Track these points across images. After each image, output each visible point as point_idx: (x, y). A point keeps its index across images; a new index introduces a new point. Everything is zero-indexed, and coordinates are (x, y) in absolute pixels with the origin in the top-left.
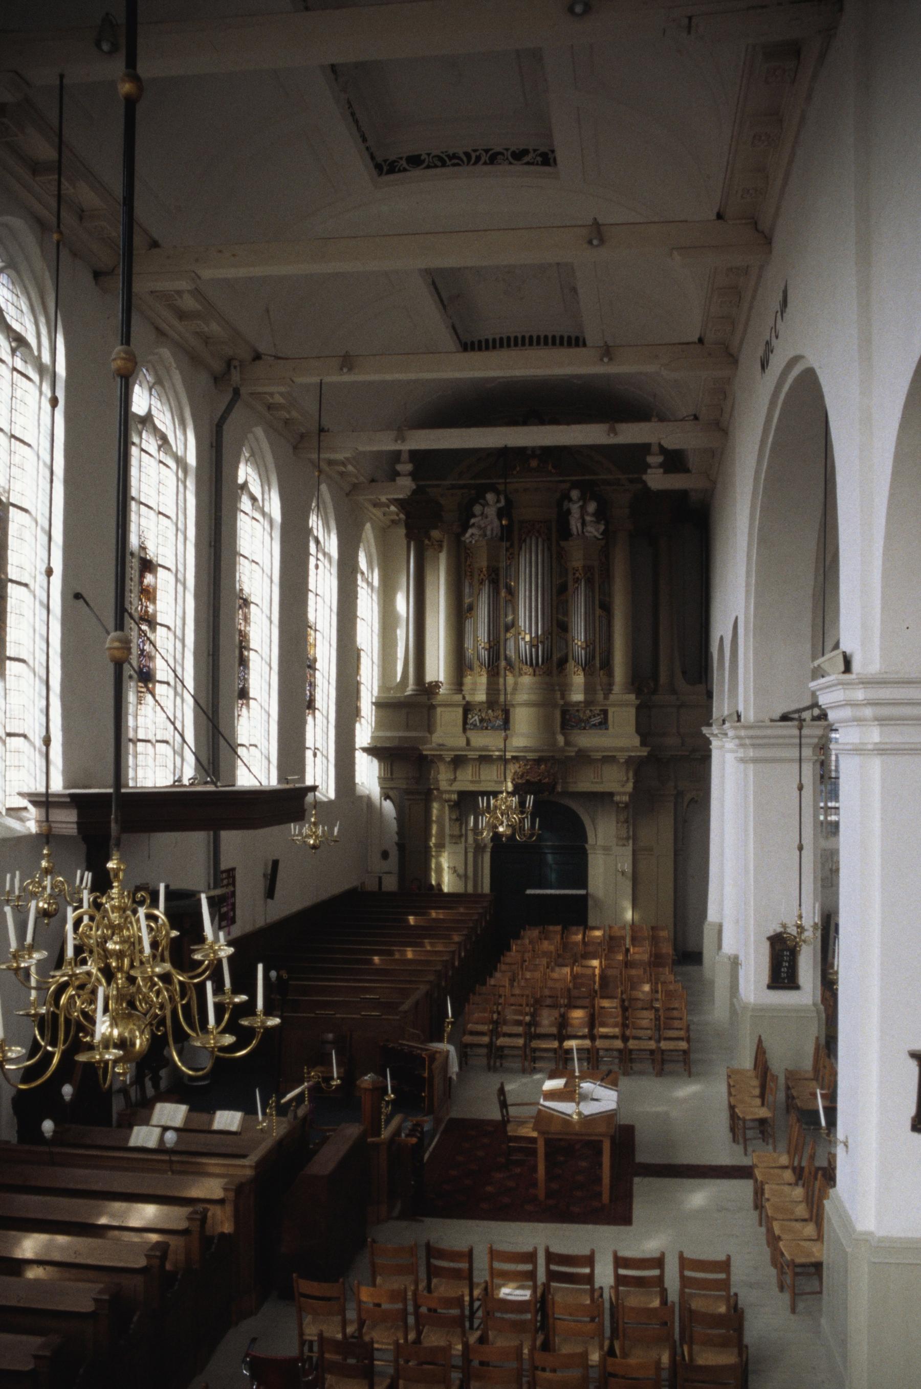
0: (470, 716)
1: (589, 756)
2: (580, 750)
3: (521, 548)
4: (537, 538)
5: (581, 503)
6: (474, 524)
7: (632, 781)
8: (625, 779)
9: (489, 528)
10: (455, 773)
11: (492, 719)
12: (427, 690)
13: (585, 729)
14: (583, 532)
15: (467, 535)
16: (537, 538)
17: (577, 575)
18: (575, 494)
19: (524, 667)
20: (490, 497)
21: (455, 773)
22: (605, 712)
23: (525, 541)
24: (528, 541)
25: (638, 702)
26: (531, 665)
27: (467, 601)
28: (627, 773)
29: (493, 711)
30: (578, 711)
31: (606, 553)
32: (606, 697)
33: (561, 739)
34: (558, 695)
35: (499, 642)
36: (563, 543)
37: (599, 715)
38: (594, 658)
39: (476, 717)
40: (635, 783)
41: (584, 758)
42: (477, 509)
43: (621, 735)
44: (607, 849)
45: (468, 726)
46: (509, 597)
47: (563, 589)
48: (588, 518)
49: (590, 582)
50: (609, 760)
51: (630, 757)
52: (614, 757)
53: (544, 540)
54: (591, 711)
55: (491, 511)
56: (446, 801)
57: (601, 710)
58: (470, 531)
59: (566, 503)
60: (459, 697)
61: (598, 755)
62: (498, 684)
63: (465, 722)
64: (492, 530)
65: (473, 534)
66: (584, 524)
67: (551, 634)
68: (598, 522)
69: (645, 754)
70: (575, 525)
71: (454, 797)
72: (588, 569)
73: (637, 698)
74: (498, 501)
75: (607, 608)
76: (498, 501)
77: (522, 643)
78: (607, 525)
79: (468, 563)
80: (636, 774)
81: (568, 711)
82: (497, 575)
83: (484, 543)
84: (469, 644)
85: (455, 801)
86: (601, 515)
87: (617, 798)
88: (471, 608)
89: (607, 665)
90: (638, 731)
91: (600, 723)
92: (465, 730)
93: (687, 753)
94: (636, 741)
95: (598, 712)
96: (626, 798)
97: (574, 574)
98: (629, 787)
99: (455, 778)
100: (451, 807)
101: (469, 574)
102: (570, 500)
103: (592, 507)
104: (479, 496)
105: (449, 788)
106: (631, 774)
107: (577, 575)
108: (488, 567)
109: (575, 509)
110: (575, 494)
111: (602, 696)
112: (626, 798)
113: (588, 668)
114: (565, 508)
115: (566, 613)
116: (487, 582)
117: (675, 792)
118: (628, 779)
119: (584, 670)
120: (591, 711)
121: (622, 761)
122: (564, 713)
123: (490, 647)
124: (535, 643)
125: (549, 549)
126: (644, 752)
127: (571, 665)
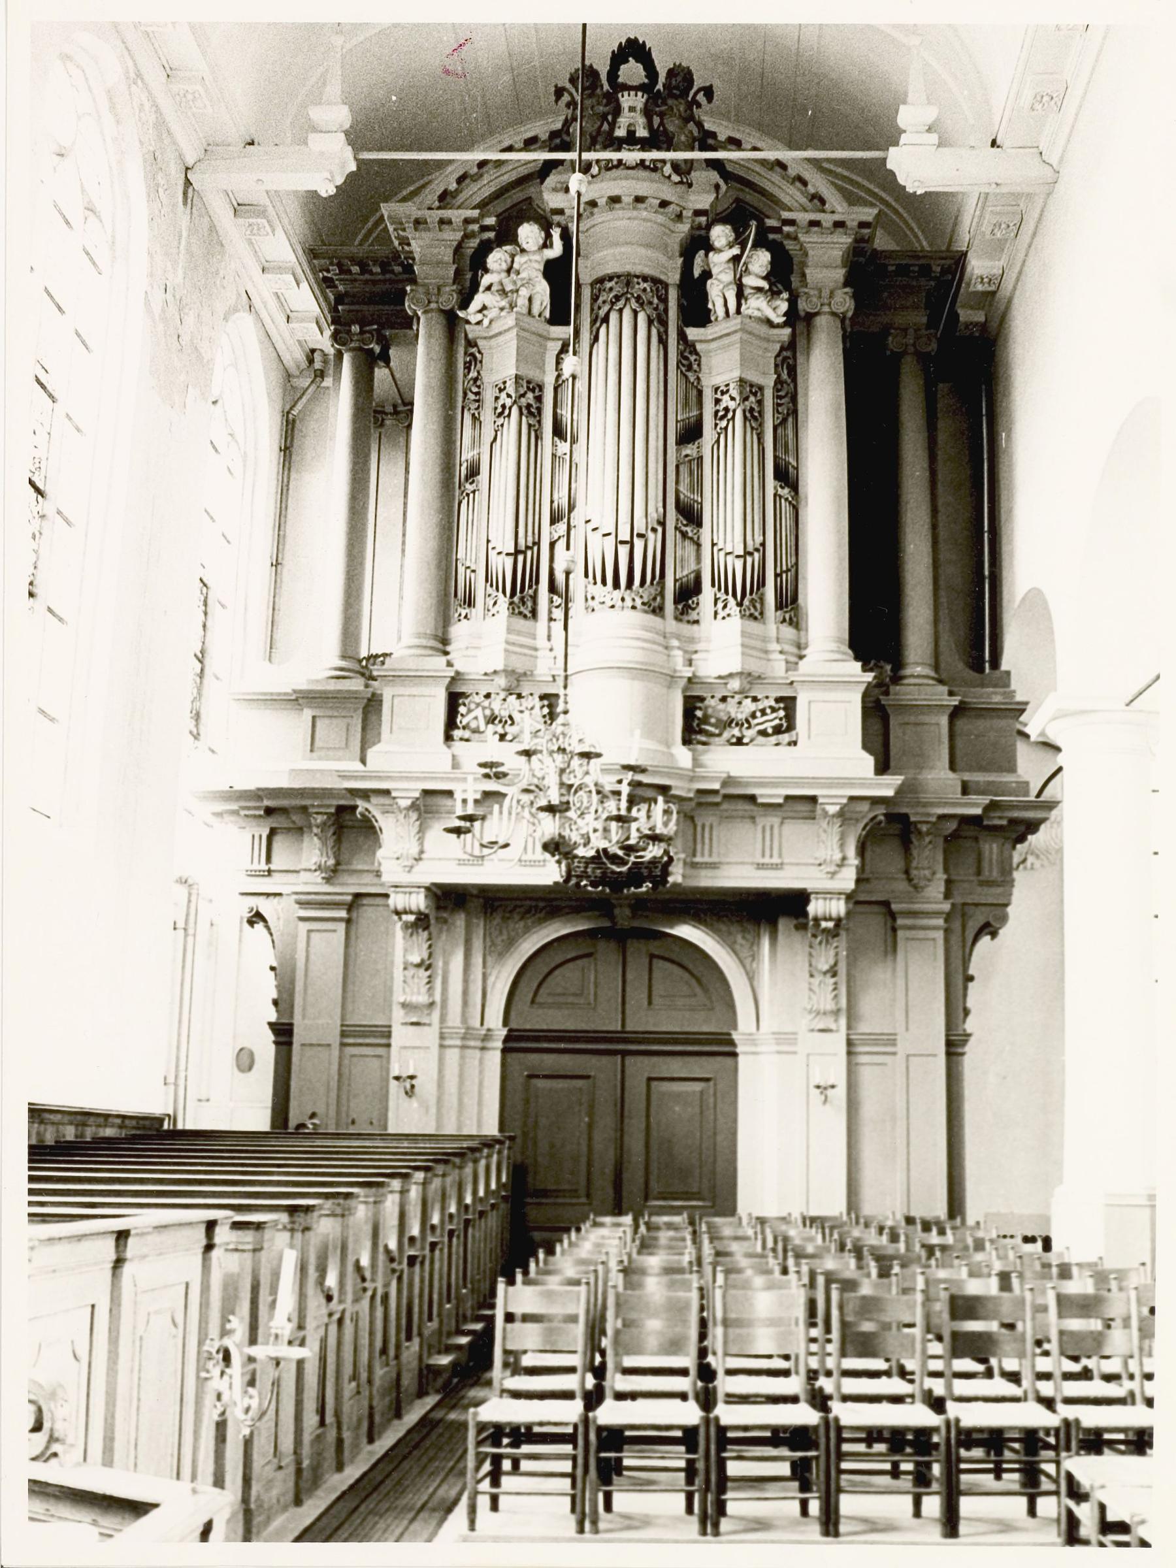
0: (462, 710)
1: (752, 799)
2: (728, 781)
3: (596, 339)
4: (635, 313)
5: (736, 251)
6: (489, 288)
7: (854, 861)
8: (838, 856)
9: (524, 292)
10: (421, 840)
11: (516, 716)
12: (365, 667)
13: (739, 742)
14: (738, 312)
15: (475, 305)
16: (635, 313)
17: (726, 401)
18: (720, 234)
19: (598, 590)
20: (529, 233)
21: (421, 840)
22: (789, 704)
23: (606, 320)
24: (614, 317)
25: (869, 677)
26: (616, 585)
27: (467, 455)
28: (842, 846)
29: (519, 696)
30: (724, 699)
31: (789, 363)
32: (791, 666)
33: (683, 756)
34: (678, 657)
35: (537, 543)
36: (692, 333)
37: (774, 710)
38: (762, 583)
39: (478, 712)
40: (861, 869)
41: (737, 801)
42: (497, 259)
43: (830, 749)
44: (785, 1039)
45: (457, 734)
46: (563, 447)
47: (691, 433)
48: (750, 281)
49: (753, 417)
50: (803, 805)
51: (852, 799)
52: (813, 799)
53: (650, 322)
54: (755, 699)
55: (531, 267)
56: (397, 913)
57: (778, 700)
58: (479, 300)
59: (702, 253)
60: (443, 660)
61: (775, 795)
62: (534, 637)
63: (451, 723)
64: (530, 300)
65: (484, 308)
66: (740, 295)
67: (662, 523)
68: (773, 293)
69: (890, 793)
70: (719, 291)
71: (419, 901)
72: (749, 389)
73: (865, 670)
74: (547, 244)
75: (787, 476)
76: (547, 244)
77: (595, 540)
78: (793, 302)
79: (473, 374)
80: (862, 850)
81: (702, 699)
82: (539, 399)
83: (510, 320)
84: (469, 552)
85: (419, 913)
86: (784, 275)
87: (815, 908)
88: (473, 472)
89: (790, 602)
90: (866, 746)
91: (778, 730)
92: (448, 738)
93: (978, 811)
94: (868, 762)
95: (773, 703)
96: (838, 907)
97: (717, 401)
98: (847, 880)
99: (422, 852)
100: (407, 926)
101: (471, 396)
102: (709, 248)
103: (761, 261)
104: (506, 235)
105: (405, 878)
106: (851, 851)
107: (726, 401)
108: (518, 378)
109: (719, 262)
110: (720, 234)
111: (783, 664)
112: (838, 907)
113: (748, 599)
114: (697, 273)
115: (697, 485)
116: (515, 411)
117: (946, 907)
118: (844, 859)
119: (740, 604)
120: (755, 699)
121: (833, 809)
122: (691, 705)
123: (517, 552)
124: (625, 535)
125: (663, 342)
126: (887, 786)
127: (708, 593)
